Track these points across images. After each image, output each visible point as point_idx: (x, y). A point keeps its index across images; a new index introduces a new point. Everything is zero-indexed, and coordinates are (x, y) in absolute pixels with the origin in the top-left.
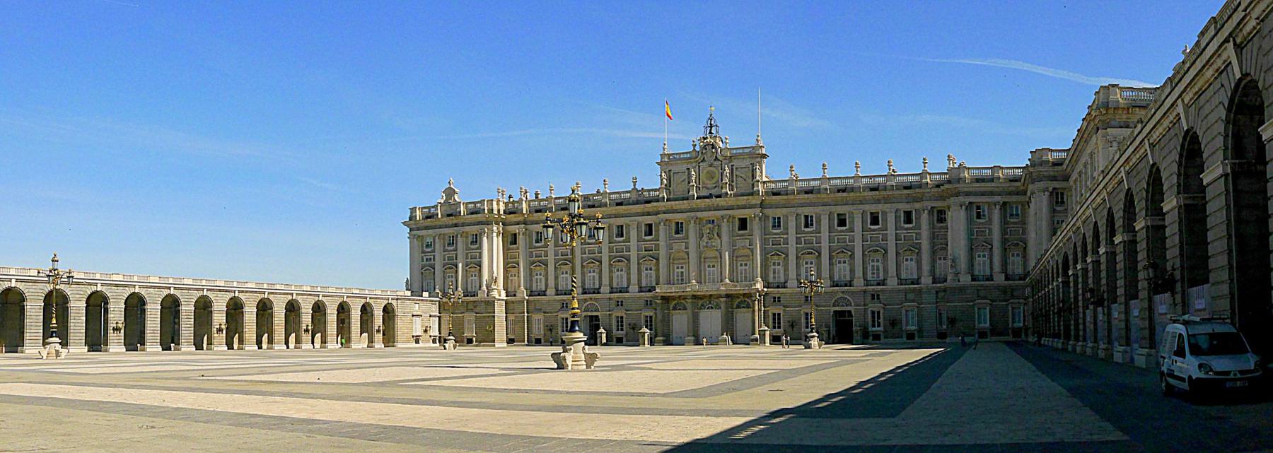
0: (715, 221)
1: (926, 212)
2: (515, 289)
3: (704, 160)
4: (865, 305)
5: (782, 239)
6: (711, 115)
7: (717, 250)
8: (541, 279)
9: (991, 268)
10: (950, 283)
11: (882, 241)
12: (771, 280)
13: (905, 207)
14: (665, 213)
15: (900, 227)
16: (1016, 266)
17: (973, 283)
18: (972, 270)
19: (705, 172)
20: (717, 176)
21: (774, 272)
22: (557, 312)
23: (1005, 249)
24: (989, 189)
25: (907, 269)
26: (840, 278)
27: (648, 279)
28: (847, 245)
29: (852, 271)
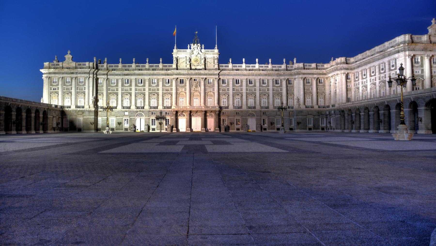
1: (285, 80)
4: (260, 116)
7: (199, 92)
8: (114, 101)
11: (267, 91)
13: (275, 78)
14: (176, 75)
15: (274, 85)
16: (321, 103)
17: (306, 109)
20: (199, 61)
21: (223, 102)
22: (123, 116)
24: (312, 72)
25: (277, 102)
26: (250, 105)
27: (167, 103)
28: (253, 92)
29: (255, 102)
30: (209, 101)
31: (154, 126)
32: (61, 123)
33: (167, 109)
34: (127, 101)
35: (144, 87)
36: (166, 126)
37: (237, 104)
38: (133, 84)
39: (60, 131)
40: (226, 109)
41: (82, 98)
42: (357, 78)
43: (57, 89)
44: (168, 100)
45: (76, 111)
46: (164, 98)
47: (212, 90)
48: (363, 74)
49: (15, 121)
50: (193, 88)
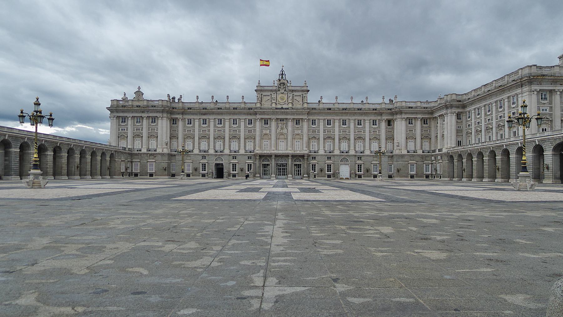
0: (285, 120)
1: (384, 121)
2: (175, 148)
3: (279, 90)
5: (317, 130)
6: (282, 69)
8: (190, 144)
9: (415, 147)
10: (396, 152)
12: (311, 149)
14: (260, 115)
16: (426, 147)
17: (408, 153)
18: (407, 148)
19: (279, 96)
21: (313, 146)
23: (422, 138)
27: (250, 146)
29: (349, 146)
30: (297, 144)
31: (234, 172)
32: (130, 167)
33: (249, 153)
34: (205, 144)
35: (224, 128)
36: (248, 172)
37: (328, 148)
38: (212, 124)
39: (129, 176)
40: (316, 154)
41: (154, 140)
42: (469, 117)
43: (126, 130)
44: (251, 143)
45: (147, 154)
46: (246, 141)
47: (300, 132)
48: (477, 113)
49: (79, 165)
50: (278, 131)
